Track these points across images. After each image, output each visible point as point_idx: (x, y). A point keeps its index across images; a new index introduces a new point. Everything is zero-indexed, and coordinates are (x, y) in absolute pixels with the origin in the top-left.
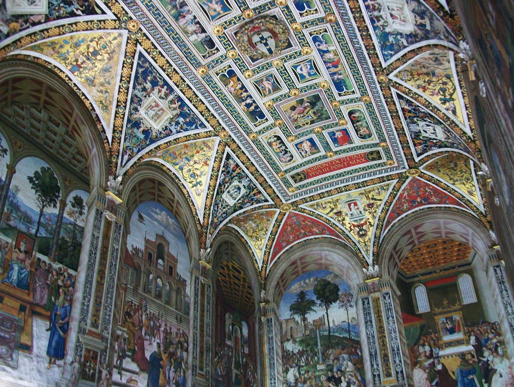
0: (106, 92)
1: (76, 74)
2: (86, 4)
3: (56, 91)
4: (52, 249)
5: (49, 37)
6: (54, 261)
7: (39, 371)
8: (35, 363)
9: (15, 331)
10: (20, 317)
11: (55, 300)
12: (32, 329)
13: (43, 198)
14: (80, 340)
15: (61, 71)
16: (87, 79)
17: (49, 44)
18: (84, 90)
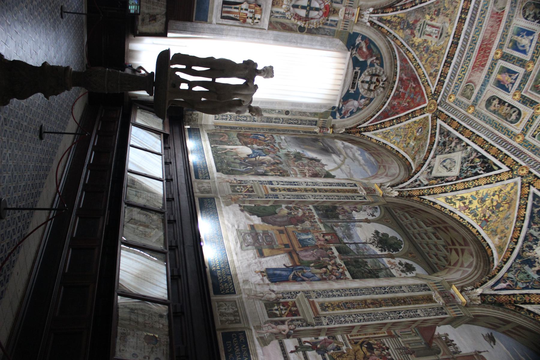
0: (505, 236)
1: (484, 228)
2: (487, 165)
3: (458, 232)
4: (348, 256)
5: (456, 190)
6: (342, 259)
7: (249, 265)
8: (254, 261)
9: (267, 244)
10: (280, 245)
11: (313, 266)
12: (277, 255)
13: (376, 242)
14: (298, 295)
15: (473, 227)
16: (492, 231)
17: (459, 198)
18: (489, 241)
